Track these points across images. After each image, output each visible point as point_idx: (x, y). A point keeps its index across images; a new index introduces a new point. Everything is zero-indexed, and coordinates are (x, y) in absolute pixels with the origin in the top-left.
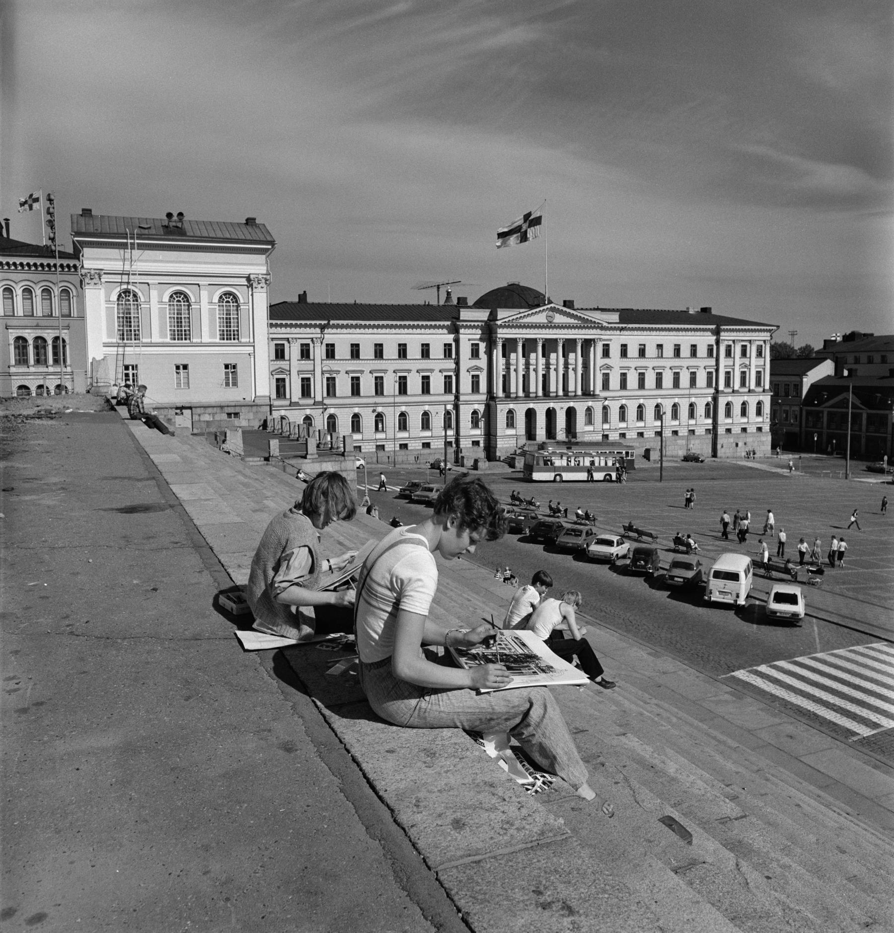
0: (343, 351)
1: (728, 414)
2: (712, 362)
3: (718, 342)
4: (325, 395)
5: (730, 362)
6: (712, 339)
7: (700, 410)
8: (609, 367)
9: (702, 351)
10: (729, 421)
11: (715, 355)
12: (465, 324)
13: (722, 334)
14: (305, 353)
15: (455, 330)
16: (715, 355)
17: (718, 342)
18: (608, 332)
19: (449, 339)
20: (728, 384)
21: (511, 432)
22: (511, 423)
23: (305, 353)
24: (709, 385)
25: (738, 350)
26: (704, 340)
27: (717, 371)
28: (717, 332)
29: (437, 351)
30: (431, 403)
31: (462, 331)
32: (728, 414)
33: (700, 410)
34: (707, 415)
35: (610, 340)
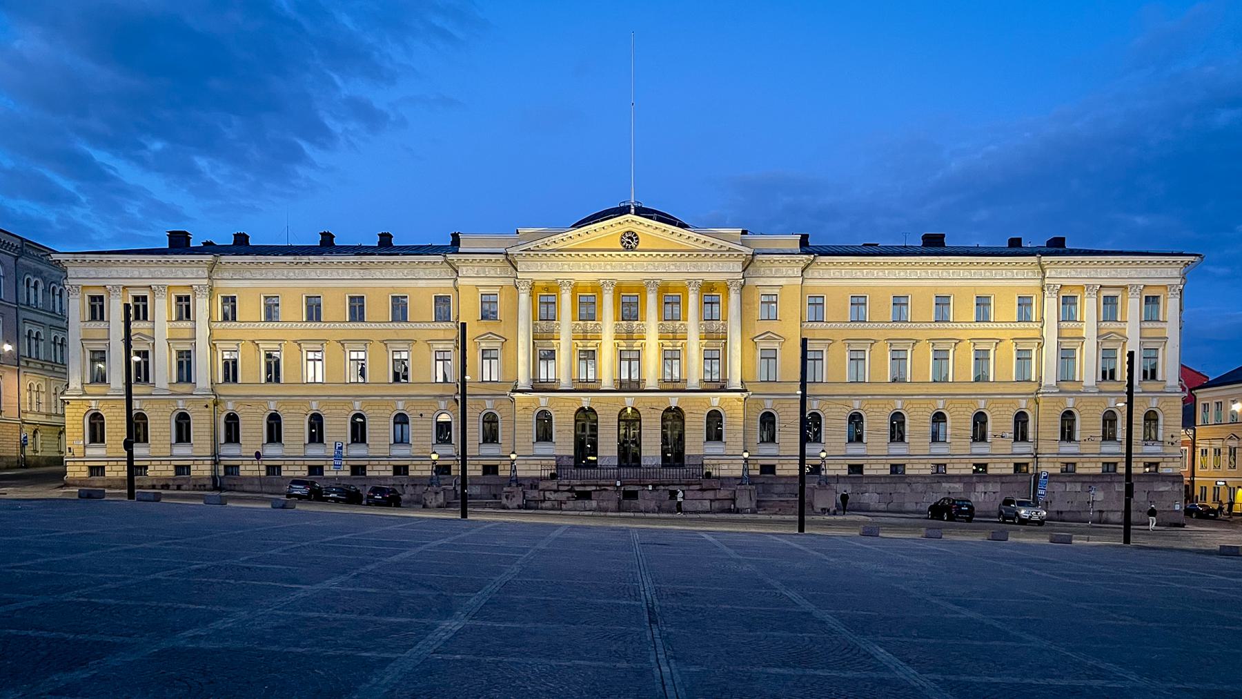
0: (250, 309)
14: (185, 308)
19: (444, 286)
21: (544, 449)
22: (545, 433)
23: (185, 308)
31: (463, 271)
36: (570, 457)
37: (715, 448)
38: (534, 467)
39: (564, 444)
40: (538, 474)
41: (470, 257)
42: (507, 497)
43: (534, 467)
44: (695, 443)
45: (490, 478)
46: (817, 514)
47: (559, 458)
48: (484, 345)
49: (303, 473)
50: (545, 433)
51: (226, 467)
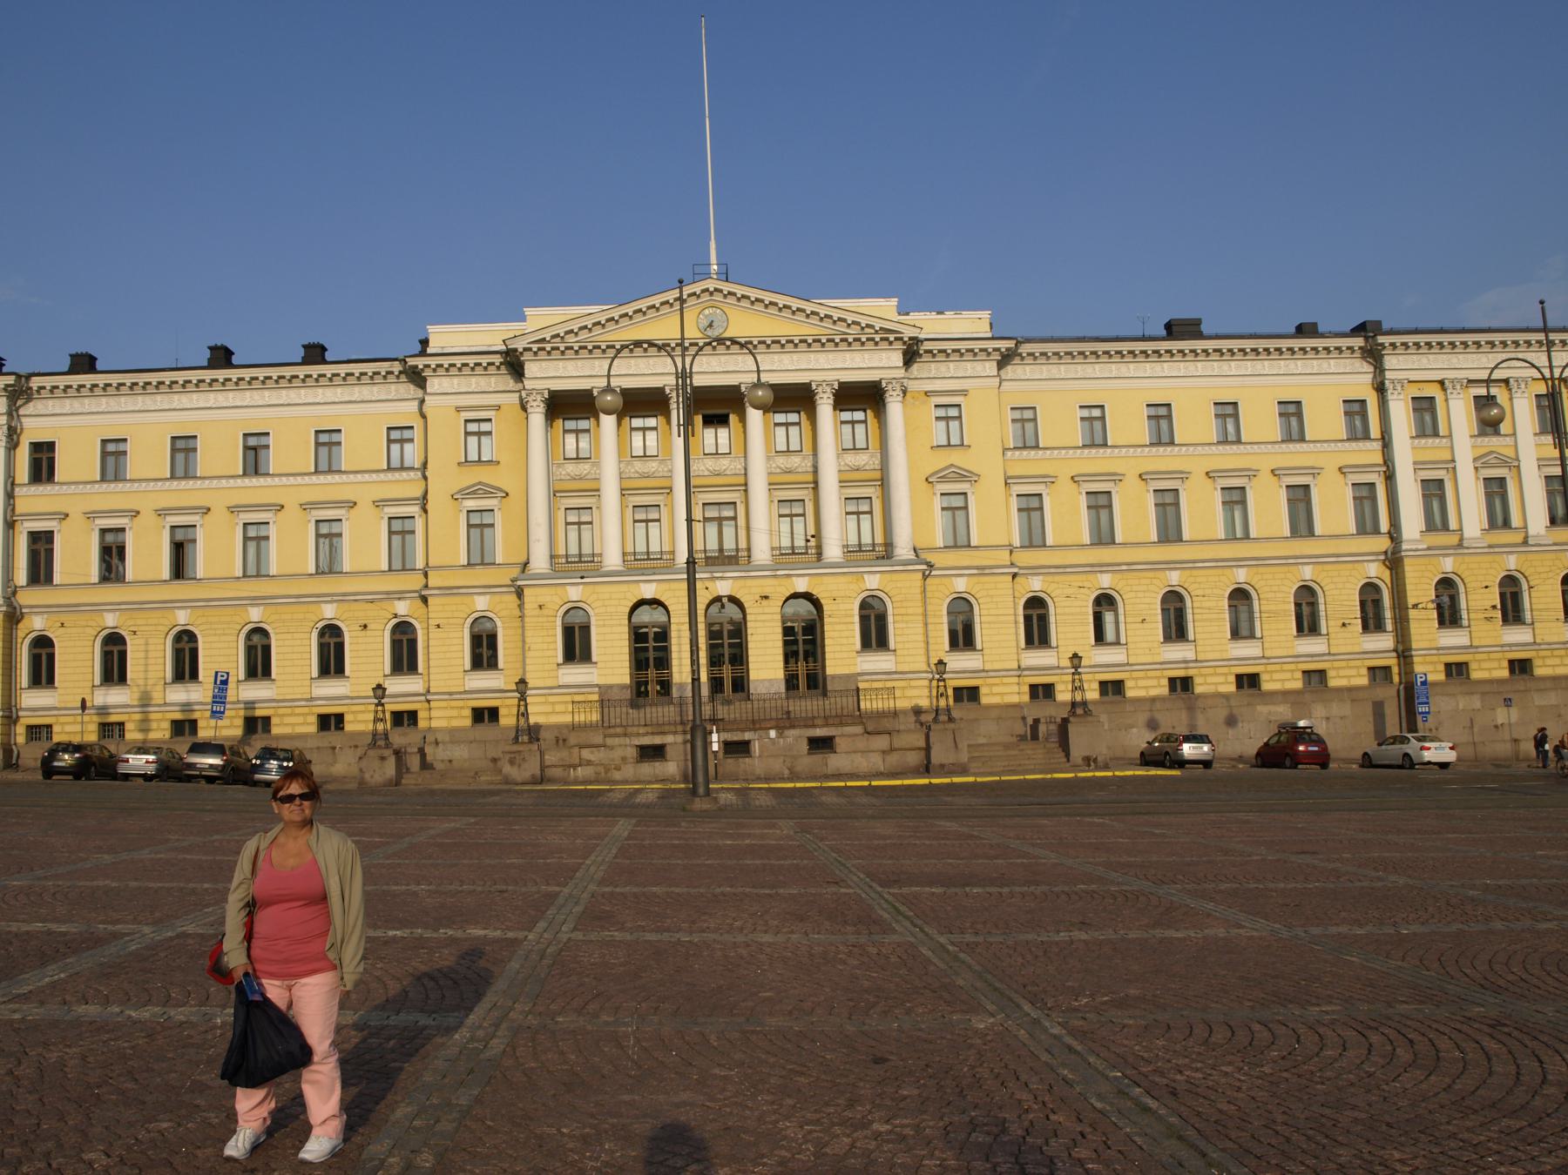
0: (77, 460)
1: (1449, 615)
2: (1369, 452)
3: (1380, 389)
4: (21, 576)
5: (1433, 449)
6: (1355, 379)
7: (1339, 602)
8: (964, 476)
9: (1325, 420)
10: (1453, 638)
11: (1375, 431)
12: (433, 362)
13: (1390, 361)
15: (417, 378)
16: (1375, 431)
17: (1380, 389)
18: (952, 368)
19: (405, 412)
20: (1436, 521)
22: (576, 645)
24: (1367, 526)
25: (1459, 413)
26: (1328, 381)
27: (1390, 477)
28: (1373, 355)
29: (363, 445)
30: (341, 598)
31: (434, 384)
32: (1449, 615)
33: (1339, 602)
34: (1371, 620)
35: (964, 393)
36: (622, 687)
37: (877, 662)
38: (559, 708)
39: (612, 661)
40: (567, 719)
41: (446, 361)
42: (512, 762)
43: (559, 708)
44: (842, 652)
45: (485, 731)
46: (1075, 768)
47: (604, 689)
48: (471, 504)
49: (92, 737)
50: (576, 645)
51: (30, 728)
